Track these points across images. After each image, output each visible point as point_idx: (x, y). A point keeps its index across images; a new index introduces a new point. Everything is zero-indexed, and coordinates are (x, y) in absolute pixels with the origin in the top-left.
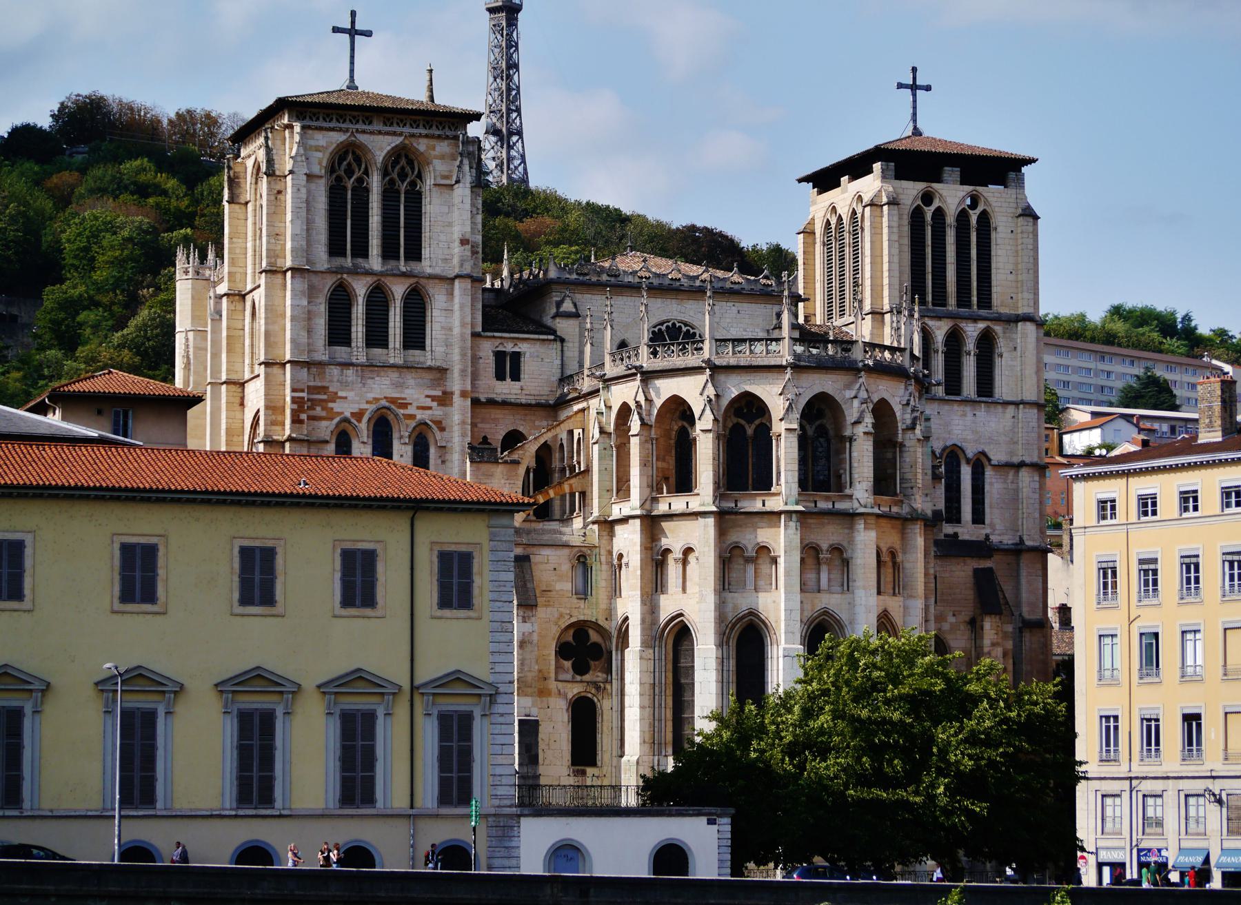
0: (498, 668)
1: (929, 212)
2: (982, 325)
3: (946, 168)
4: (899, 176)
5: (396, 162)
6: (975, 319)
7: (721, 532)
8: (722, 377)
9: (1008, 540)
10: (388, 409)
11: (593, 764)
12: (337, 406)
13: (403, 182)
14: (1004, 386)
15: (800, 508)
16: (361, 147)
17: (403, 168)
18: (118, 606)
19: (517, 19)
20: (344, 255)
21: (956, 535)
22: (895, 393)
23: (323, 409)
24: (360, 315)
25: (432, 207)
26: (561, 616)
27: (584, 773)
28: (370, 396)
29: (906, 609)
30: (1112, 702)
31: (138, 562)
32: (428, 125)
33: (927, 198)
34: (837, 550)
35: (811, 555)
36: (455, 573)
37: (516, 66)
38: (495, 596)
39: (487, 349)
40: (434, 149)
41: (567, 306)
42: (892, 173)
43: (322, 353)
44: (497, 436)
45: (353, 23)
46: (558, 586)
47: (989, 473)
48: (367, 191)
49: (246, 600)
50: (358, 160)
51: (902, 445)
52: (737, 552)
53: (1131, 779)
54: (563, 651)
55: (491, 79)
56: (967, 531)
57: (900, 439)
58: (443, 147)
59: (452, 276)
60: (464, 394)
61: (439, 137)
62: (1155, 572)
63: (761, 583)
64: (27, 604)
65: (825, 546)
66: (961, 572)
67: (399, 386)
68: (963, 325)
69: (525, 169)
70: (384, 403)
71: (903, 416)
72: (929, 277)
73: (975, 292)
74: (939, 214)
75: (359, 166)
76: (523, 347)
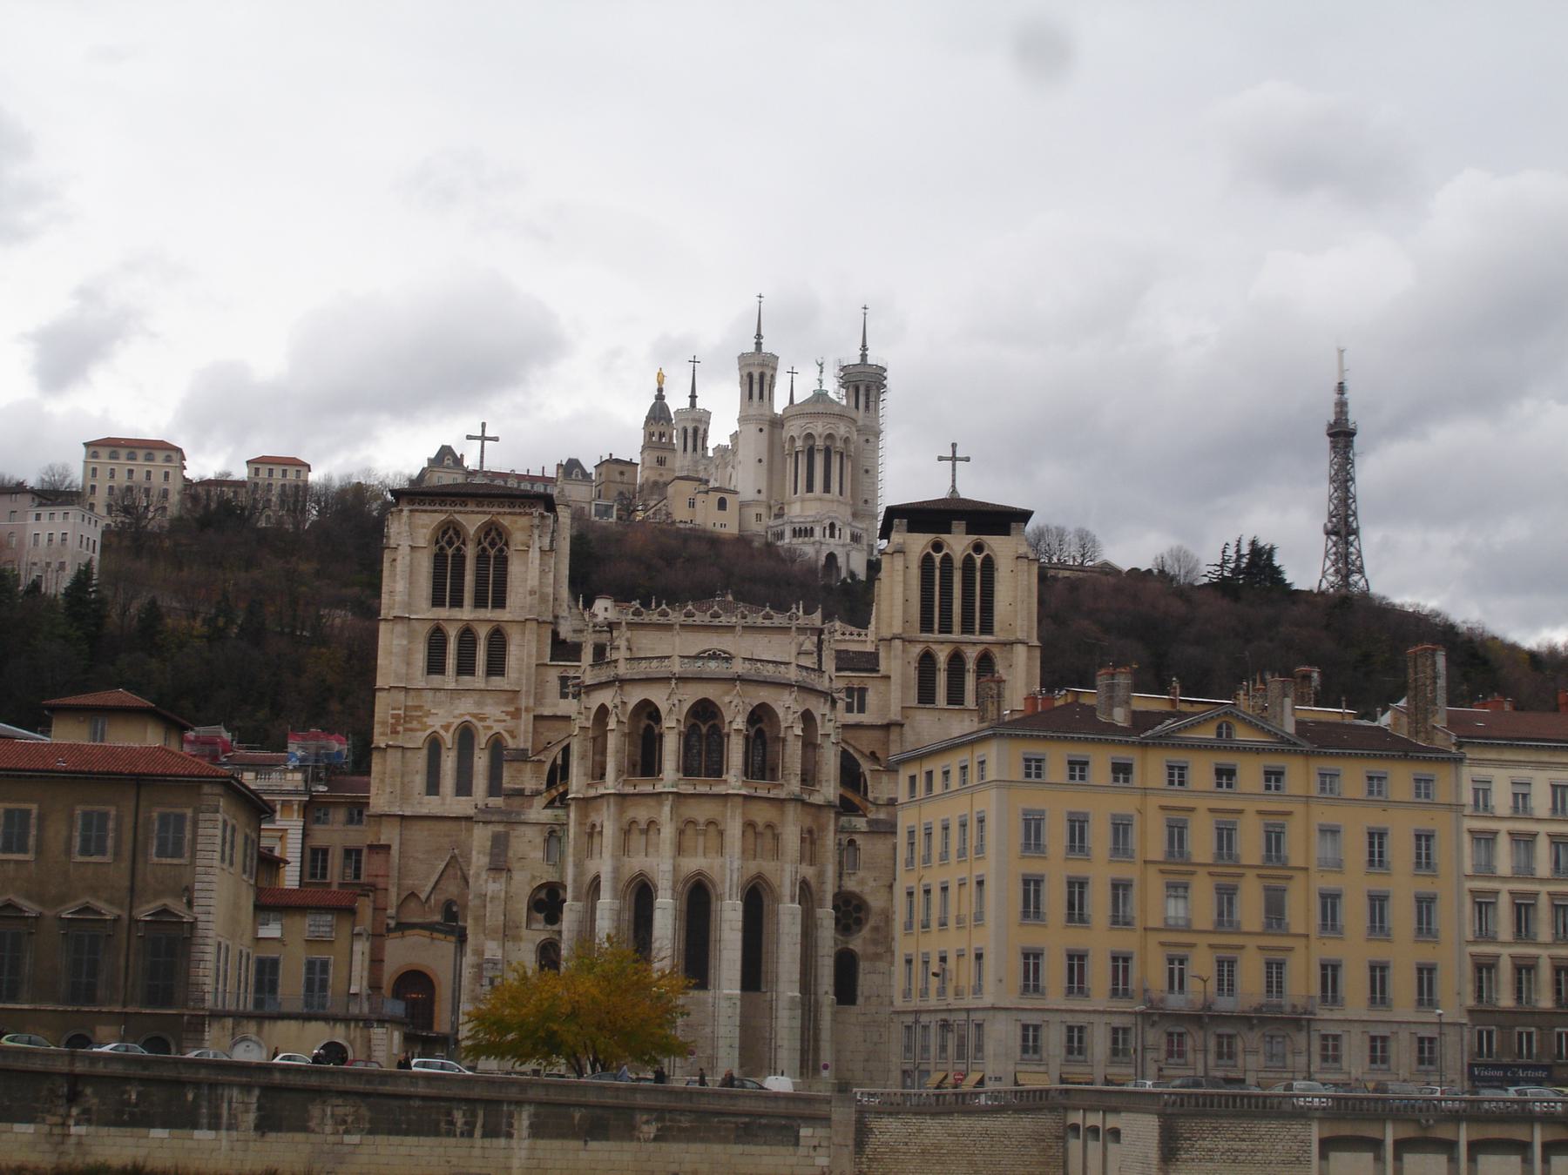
1: (938, 557)
2: (980, 648)
3: (954, 522)
4: (913, 528)
5: (487, 534)
7: (621, 811)
8: (628, 688)
10: (470, 722)
12: (429, 721)
13: (492, 549)
15: (675, 790)
16: (459, 523)
17: (493, 539)
19: (1352, 441)
20: (444, 605)
23: (420, 722)
24: (452, 652)
25: (514, 568)
26: (534, 878)
28: (457, 712)
29: (783, 870)
32: (512, 505)
33: (937, 547)
35: (685, 828)
36: (171, 830)
39: (553, 676)
40: (516, 522)
42: (905, 528)
43: (420, 679)
45: (483, 431)
46: (532, 855)
48: (463, 558)
50: (457, 533)
51: (784, 740)
52: (634, 826)
53: (916, 1012)
54: (536, 905)
55: (1332, 491)
57: (782, 735)
58: (523, 521)
59: (522, 619)
60: (527, 710)
61: (520, 514)
63: (651, 850)
65: (702, 820)
67: (479, 704)
69: (1362, 561)
70: (468, 718)
72: (937, 610)
73: (977, 621)
74: (947, 559)
75: (459, 538)
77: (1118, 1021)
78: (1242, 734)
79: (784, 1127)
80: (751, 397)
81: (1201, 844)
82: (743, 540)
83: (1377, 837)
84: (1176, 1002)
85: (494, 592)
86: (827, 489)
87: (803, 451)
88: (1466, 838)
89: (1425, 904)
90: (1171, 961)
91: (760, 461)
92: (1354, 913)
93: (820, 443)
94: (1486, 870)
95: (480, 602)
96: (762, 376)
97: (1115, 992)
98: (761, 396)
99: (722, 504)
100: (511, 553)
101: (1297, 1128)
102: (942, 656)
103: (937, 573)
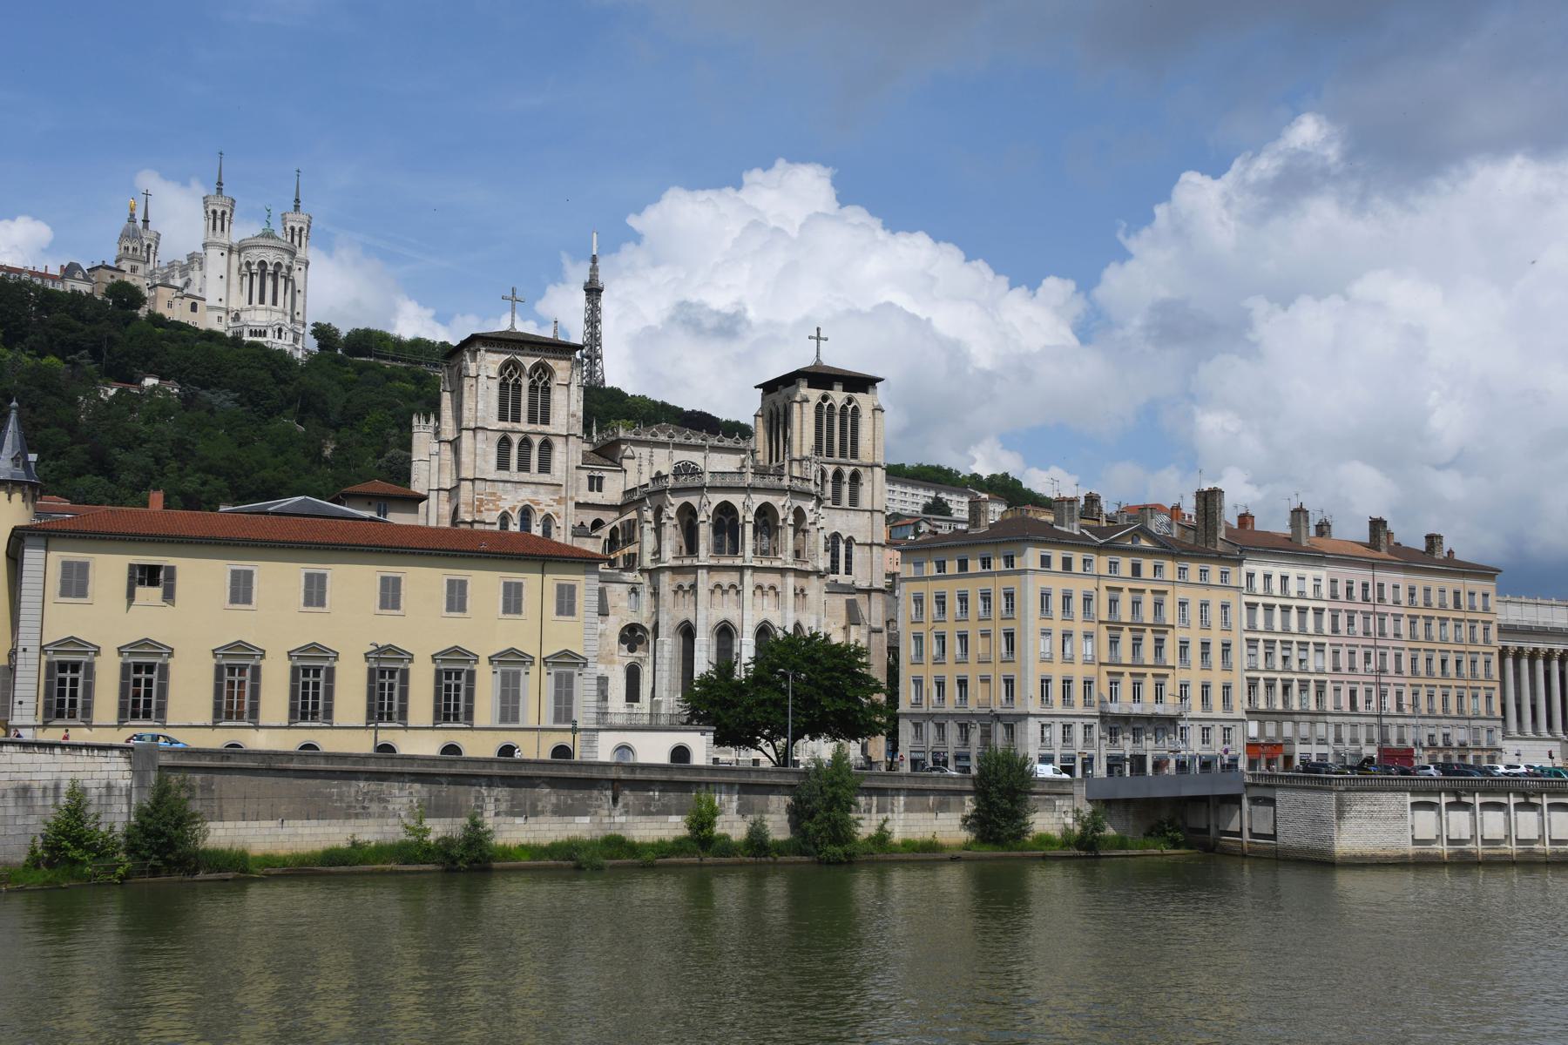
0: (589, 648)
2: (852, 468)
4: (810, 386)
6: (849, 465)
9: (864, 585)
11: (638, 701)
12: (501, 504)
14: (865, 501)
17: (540, 374)
18: (378, 611)
21: (836, 581)
22: (808, 506)
25: (558, 397)
26: (622, 620)
27: (632, 706)
28: (520, 498)
30: (918, 671)
31: (391, 587)
34: (773, 588)
37: (599, 321)
38: (586, 609)
39: (584, 474)
41: (628, 453)
44: (588, 524)
46: (621, 604)
47: (854, 547)
48: (520, 386)
49: (450, 608)
54: (623, 639)
56: (842, 578)
60: (572, 499)
62: (944, 603)
64: (327, 609)
66: (840, 602)
68: (842, 467)
70: (528, 503)
71: (810, 517)
74: (831, 406)
76: (605, 474)
77: (1087, 721)
78: (1144, 543)
79: (1048, 800)
80: (214, 228)
81: (1125, 613)
82: (211, 335)
83: (1204, 605)
84: (1114, 708)
85: (542, 413)
86: (275, 302)
87: (257, 274)
88: (1244, 607)
89: (1226, 647)
90: (1111, 683)
91: (221, 277)
92: (1195, 651)
93: (270, 269)
94: (1252, 628)
95: (532, 420)
96: (223, 213)
97: (1085, 705)
98: (223, 229)
99: (194, 308)
100: (553, 384)
101: (1400, 796)
102: (830, 470)
103: (825, 417)
